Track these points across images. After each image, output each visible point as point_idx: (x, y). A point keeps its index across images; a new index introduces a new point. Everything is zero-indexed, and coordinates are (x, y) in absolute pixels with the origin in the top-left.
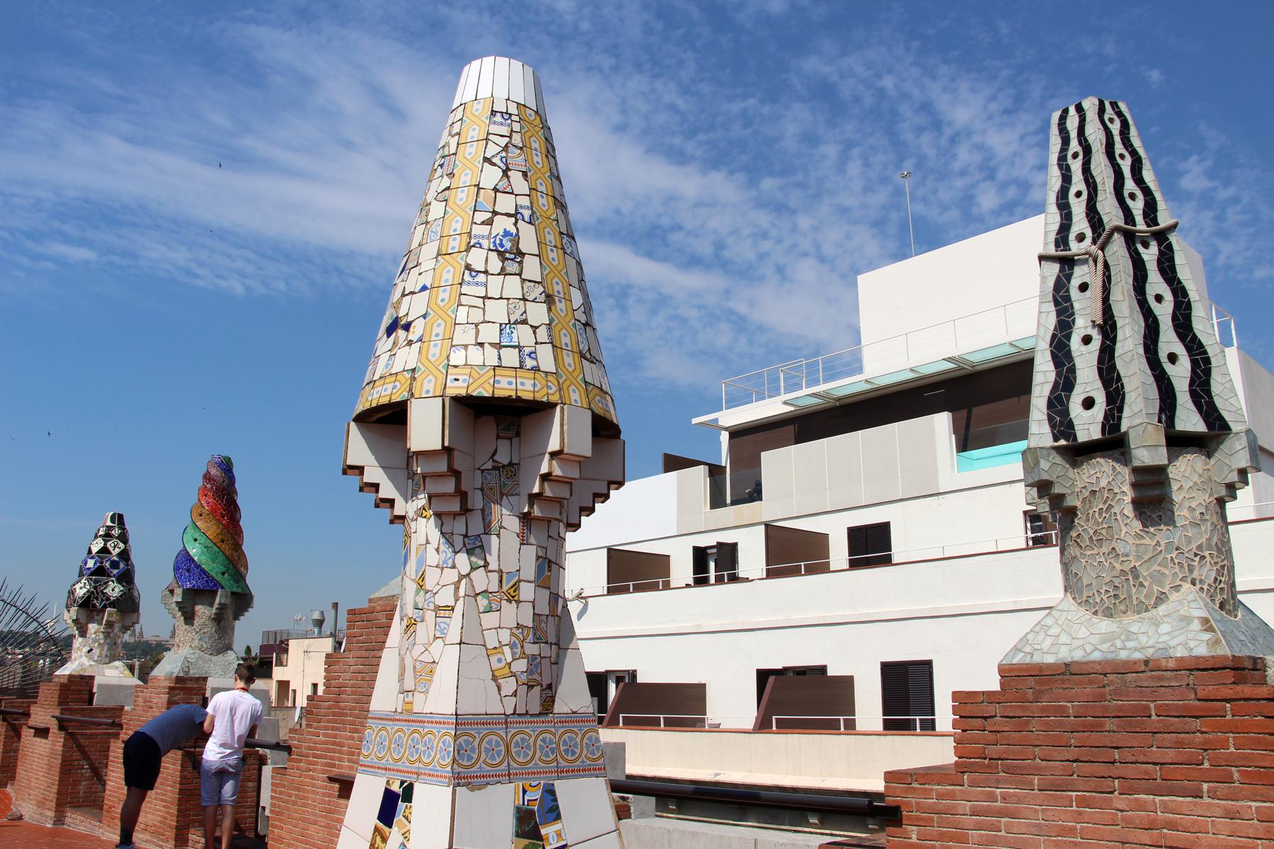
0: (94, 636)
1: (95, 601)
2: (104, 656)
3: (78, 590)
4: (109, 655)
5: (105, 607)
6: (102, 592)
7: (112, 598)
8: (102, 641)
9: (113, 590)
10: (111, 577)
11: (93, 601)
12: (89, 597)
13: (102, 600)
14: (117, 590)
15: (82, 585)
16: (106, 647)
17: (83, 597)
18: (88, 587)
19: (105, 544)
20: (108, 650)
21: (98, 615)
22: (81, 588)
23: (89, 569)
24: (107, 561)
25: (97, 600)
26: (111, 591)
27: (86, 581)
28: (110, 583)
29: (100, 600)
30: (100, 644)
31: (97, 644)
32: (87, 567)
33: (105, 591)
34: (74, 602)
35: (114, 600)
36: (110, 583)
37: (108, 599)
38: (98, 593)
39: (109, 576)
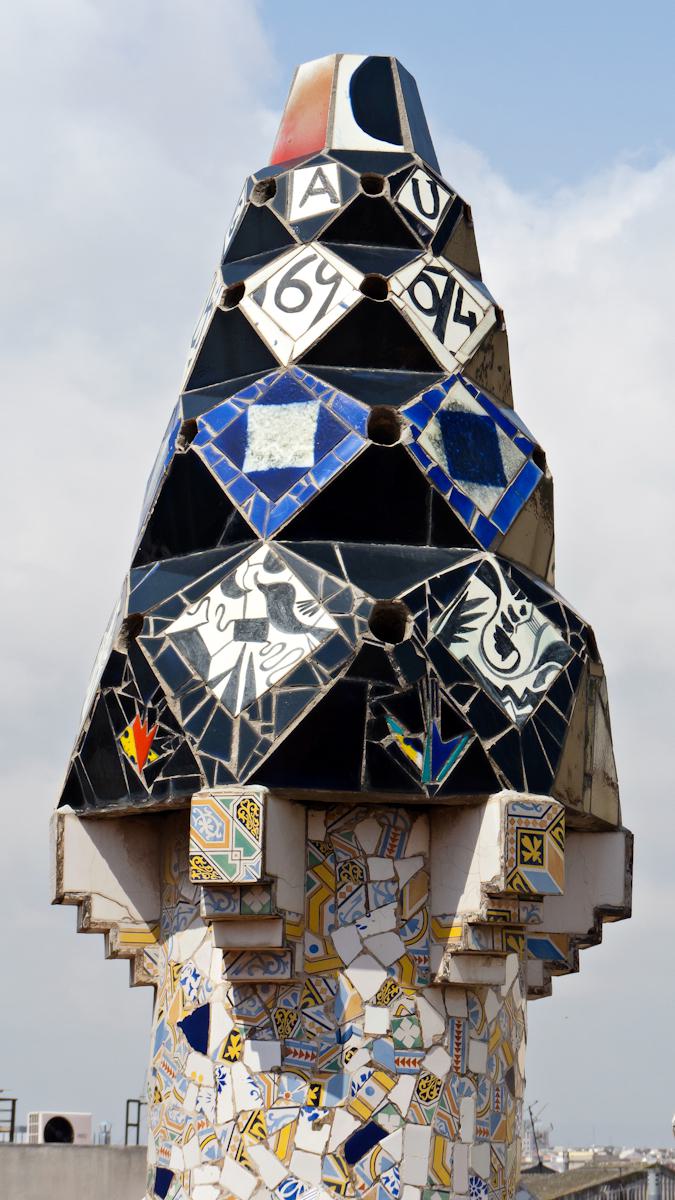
0: (377, 1020)
1: (397, 734)
2: (461, 1183)
3: (223, 653)
4: (484, 1173)
5: (475, 782)
6: (439, 651)
7: (511, 710)
8: (439, 1064)
9: (504, 646)
10: (465, 540)
11: (382, 730)
12: (343, 701)
13: (452, 724)
14: (521, 637)
15: (257, 607)
16: (468, 1106)
17: (289, 705)
18: (328, 622)
19: (374, 288)
20: (481, 1136)
21: (391, 848)
22: (247, 630)
23: (277, 480)
24: (421, 415)
25: (414, 722)
26: (494, 657)
27: (286, 576)
28: (476, 588)
29: (434, 721)
30: (426, 1088)
31: (407, 1084)
32: (251, 465)
33: (457, 651)
34: (218, 743)
35: (527, 726)
36: (476, 588)
37: (489, 715)
38: (415, 669)
39: (453, 535)
